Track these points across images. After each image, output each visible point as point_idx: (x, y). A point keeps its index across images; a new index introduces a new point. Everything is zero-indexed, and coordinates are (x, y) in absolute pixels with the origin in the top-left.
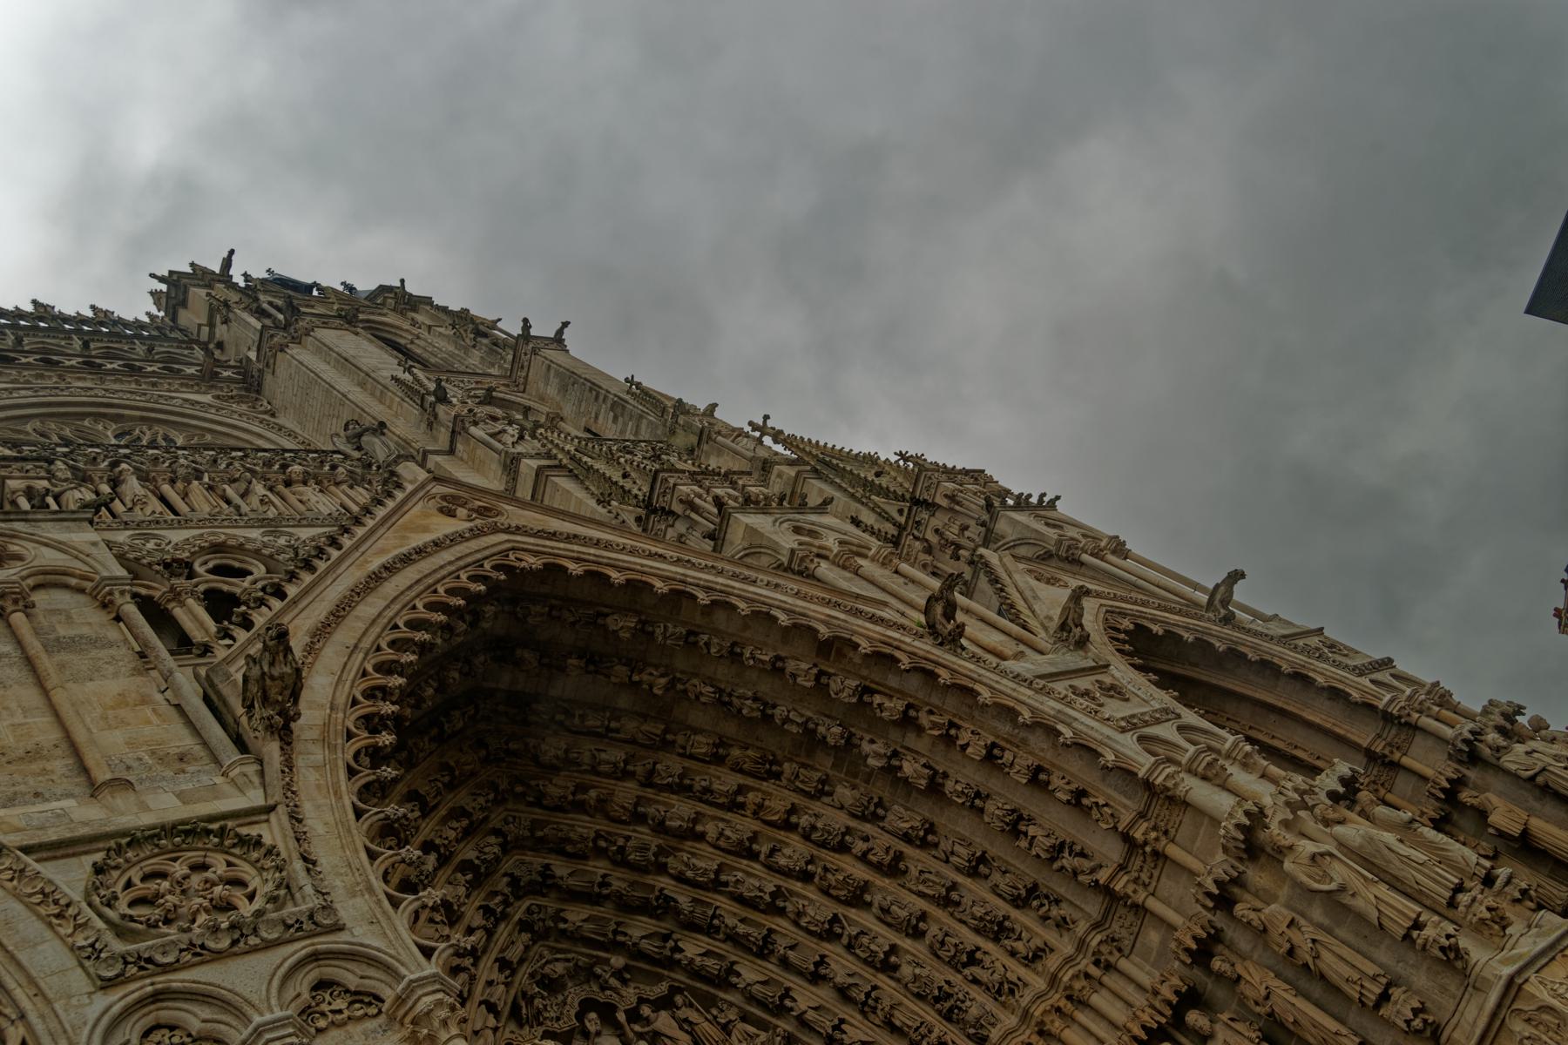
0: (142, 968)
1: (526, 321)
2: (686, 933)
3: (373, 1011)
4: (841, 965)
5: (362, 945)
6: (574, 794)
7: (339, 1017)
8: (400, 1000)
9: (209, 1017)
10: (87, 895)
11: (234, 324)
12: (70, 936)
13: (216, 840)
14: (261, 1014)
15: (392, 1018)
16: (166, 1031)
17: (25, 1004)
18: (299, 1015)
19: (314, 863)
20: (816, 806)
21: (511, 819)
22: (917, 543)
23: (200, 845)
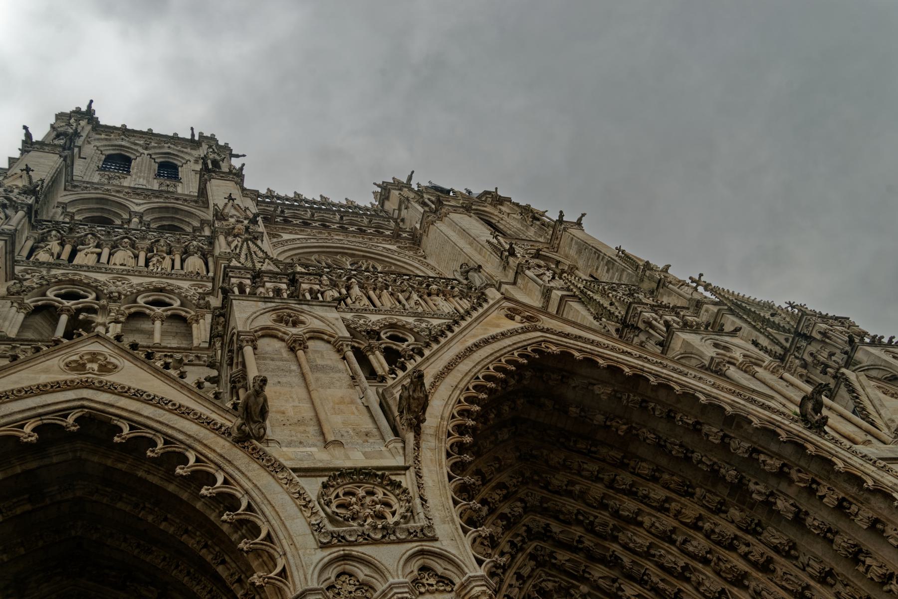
0: (339, 541)
1: (561, 212)
2: (627, 580)
3: (449, 589)
5: (446, 551)
6: (566, 486)
8: (463, 586)
9: (368, 573)
10: (318, 499)
11: (410, 210)
12: (309, 517)
13: (380, 480)
16: (347, 576)
18: (412, 582)
19: (426, 501)
20: (716, 519)
21: (530, 494)
22: (797, 361)
23: (372, 482)
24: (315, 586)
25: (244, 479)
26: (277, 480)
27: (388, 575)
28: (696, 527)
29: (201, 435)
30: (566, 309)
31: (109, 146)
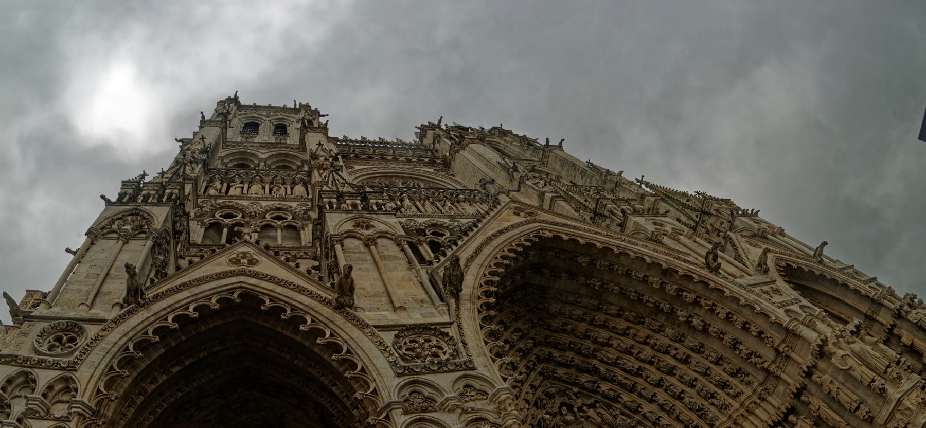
0: (409, 372)
1: (547, 139)
3: (485, 397)
4: (662, 396)
6: (562, 326)
7: (472, 398)
8: (494, 395)
9: (430, 391)
10: (393, 345)
11: (441, 143)
14: (448, 394)
15: (491, 401)
17: (375, 376)
19: (466, 345)
20: (657, 336)
22: (703, 229)
24: (397, 399)
25: (343, 333)
26: (365, 333)
27: (444, 392)
28: (645, 343)
29: (313, 305)
30: (555, 206)
31: (246, 118)
